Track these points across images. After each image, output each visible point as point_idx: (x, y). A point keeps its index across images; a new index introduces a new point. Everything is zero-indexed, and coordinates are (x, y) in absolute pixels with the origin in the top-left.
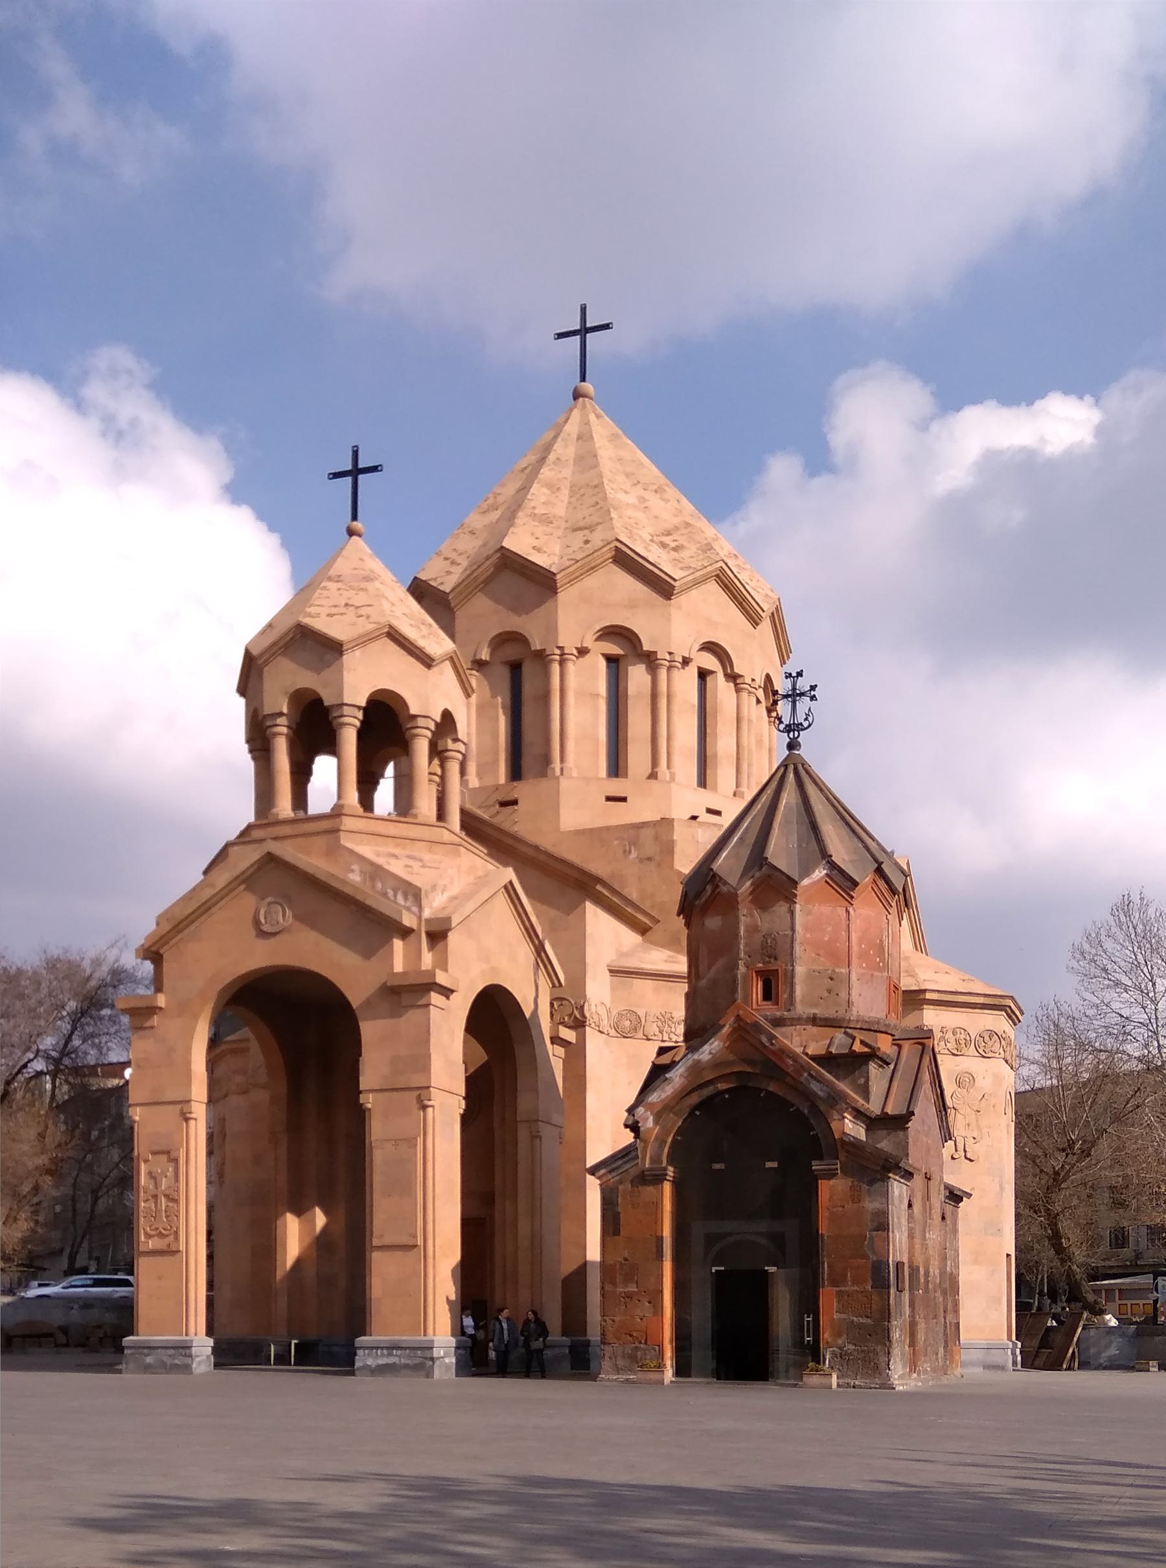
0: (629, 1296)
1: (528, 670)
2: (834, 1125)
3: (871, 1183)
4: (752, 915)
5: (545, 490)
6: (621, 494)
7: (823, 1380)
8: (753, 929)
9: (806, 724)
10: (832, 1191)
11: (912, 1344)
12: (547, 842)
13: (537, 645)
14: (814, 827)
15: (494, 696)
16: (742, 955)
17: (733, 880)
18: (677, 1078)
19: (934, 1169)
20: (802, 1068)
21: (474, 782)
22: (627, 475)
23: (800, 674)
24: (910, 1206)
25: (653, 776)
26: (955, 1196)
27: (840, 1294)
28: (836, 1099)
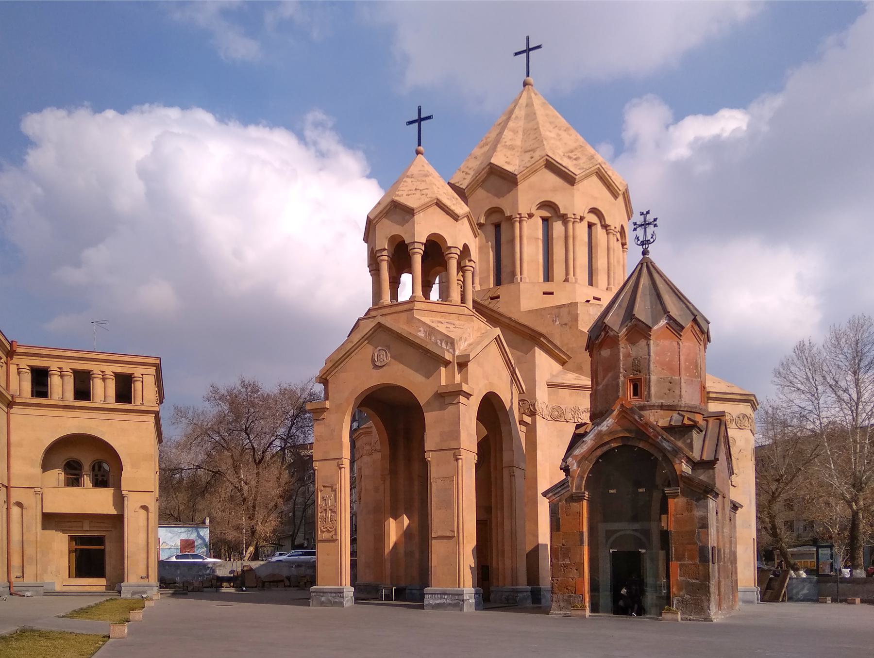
0: (566, 566)
1: (504, 227)
2: (676, 467)
3: (698, 500)
4: (627, 348)
5: (511, 133)
6: (548, 133)
7: (674, 616)
8: (628, 355)
9: (652, 240)
12: (515, 317)
13: (508, 214)
14: (659, 296)
15: (487, 242)
16: (622, 370)
17: (616, 328)
18: (589, 441)
21: (478, 288)
22: (551, 123)
23: (648, 212)
27: (681, 566)
28: (676, 451)
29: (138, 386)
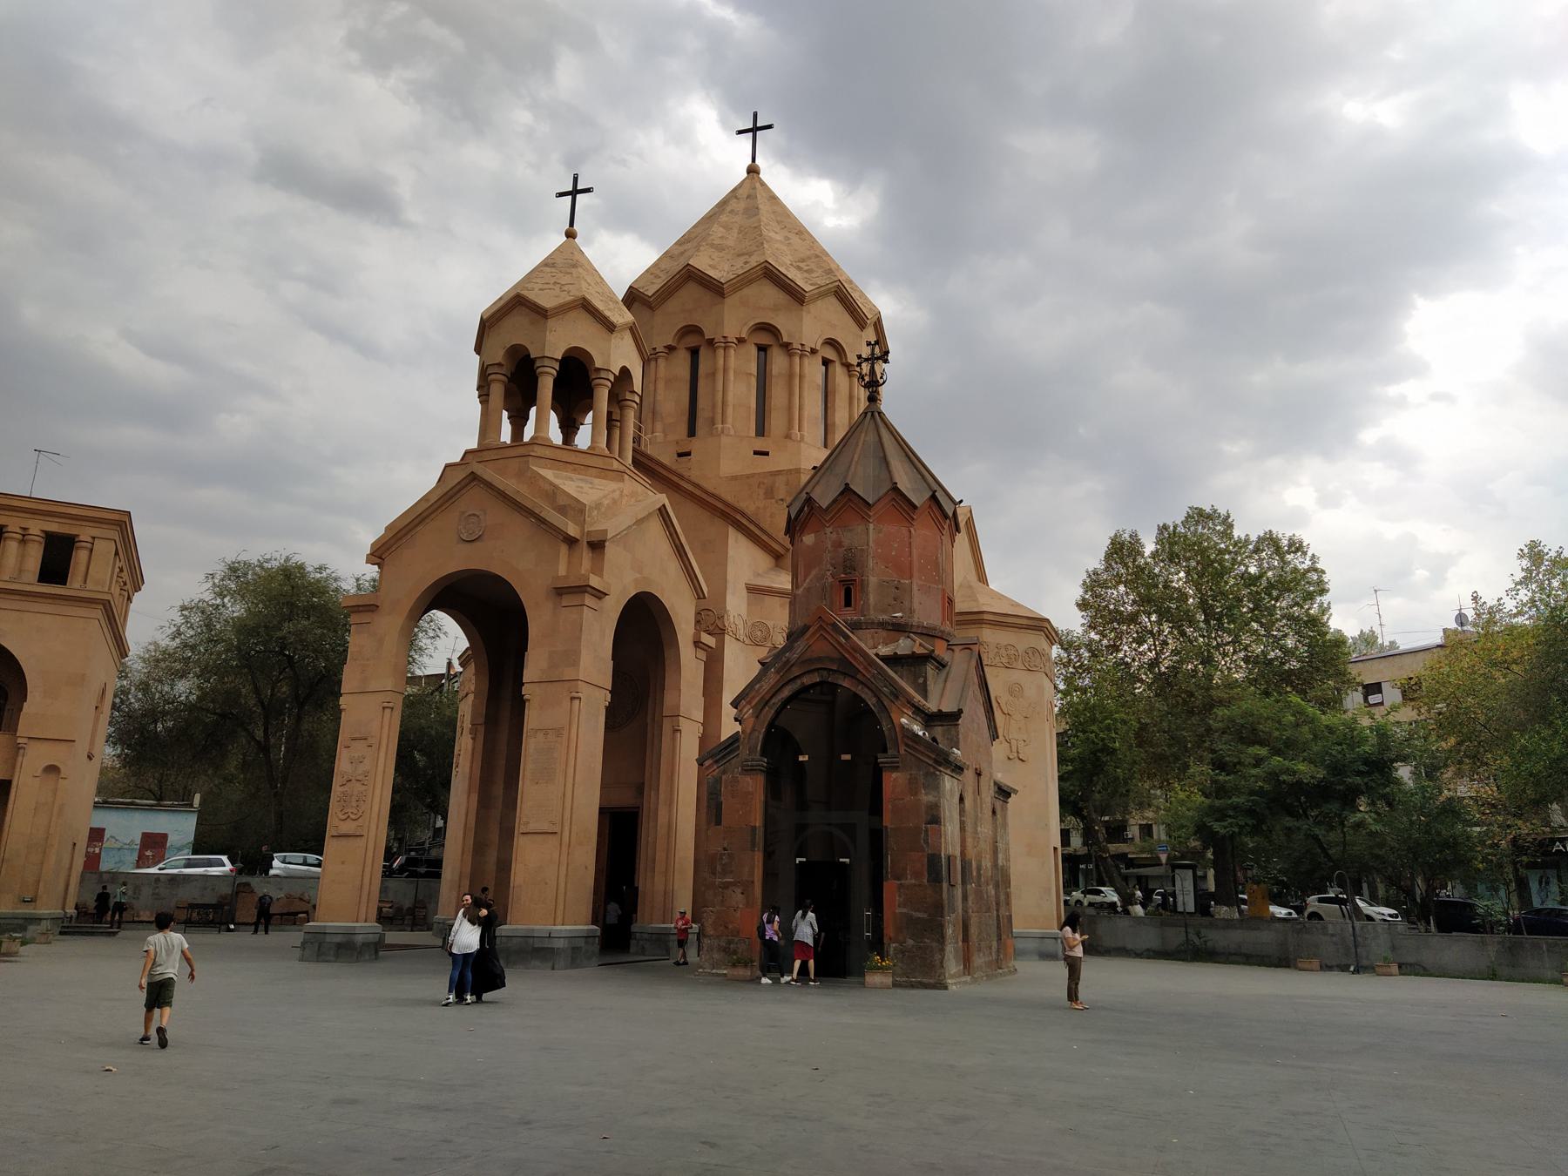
10: (893, 782)
11: (966, 939)
19: (984, 768)
20: (872, 663)
24: (961, 799)
25: (788, 437)
26: (1004, 793)
29: (80, 557)
